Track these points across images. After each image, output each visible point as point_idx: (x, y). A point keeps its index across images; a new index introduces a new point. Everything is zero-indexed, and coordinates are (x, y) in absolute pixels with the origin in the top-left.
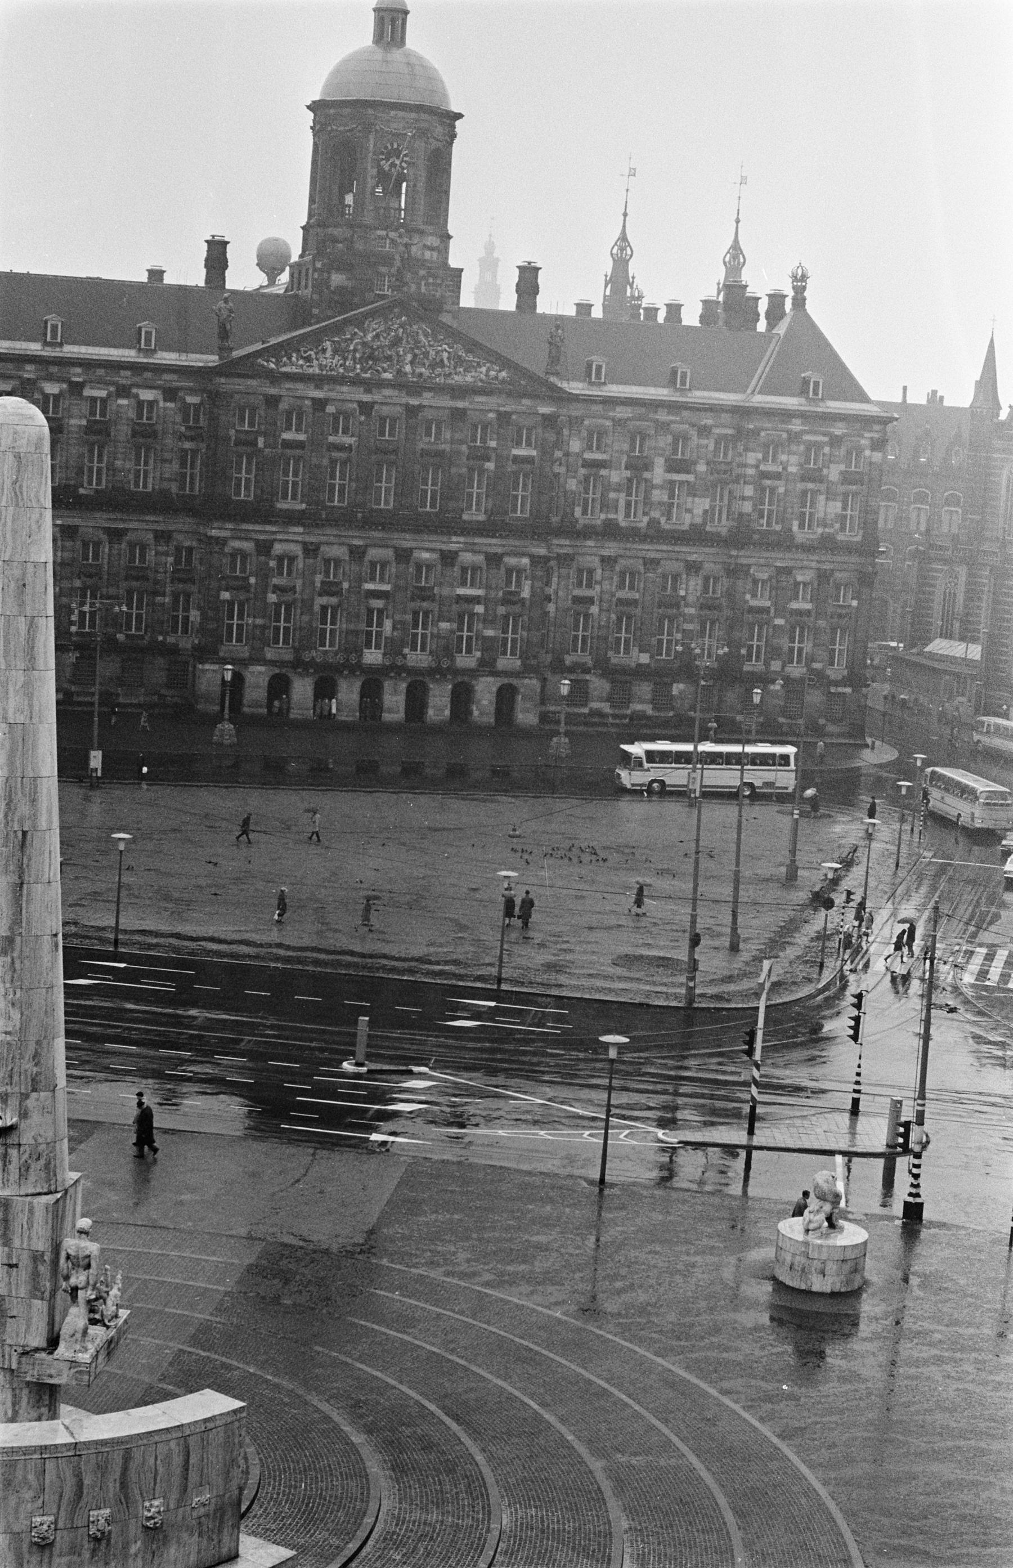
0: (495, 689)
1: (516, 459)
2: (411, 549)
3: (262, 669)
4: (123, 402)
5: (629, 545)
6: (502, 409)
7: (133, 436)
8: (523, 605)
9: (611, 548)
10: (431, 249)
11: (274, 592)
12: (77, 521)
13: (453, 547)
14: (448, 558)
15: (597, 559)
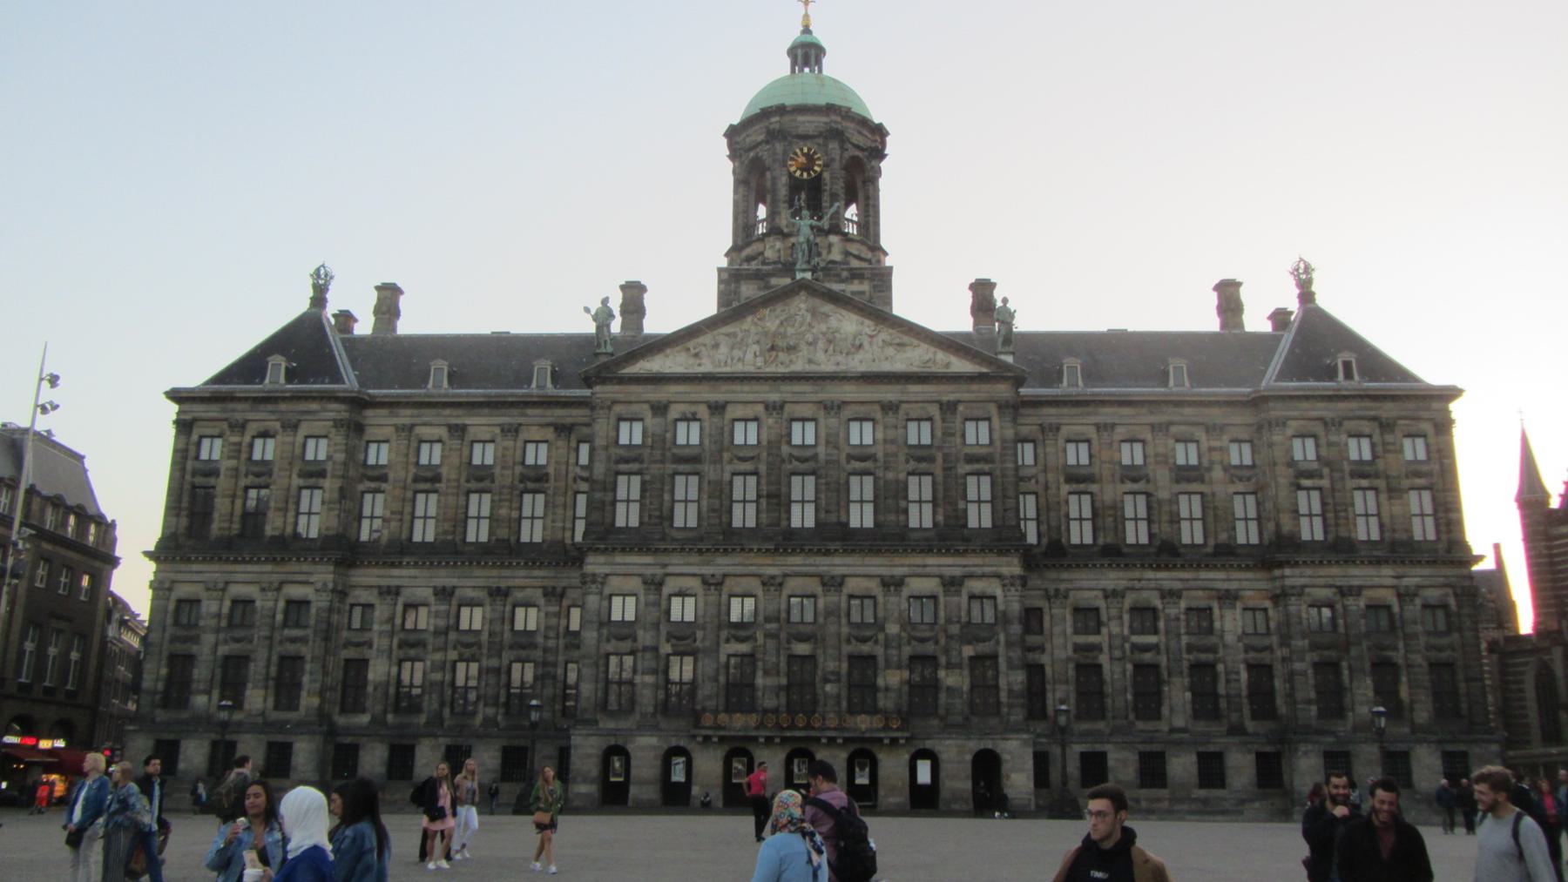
0: (969, 757)
1: (971, 459)
2: (844, 577)
3: (653, 741)
4: (510, 443)
5: (1137, 574)
6: (945, 398)
7: (521, 481)
8: (998, 643)
9: (1113, 579)
10: (858, 258)
11: (668, 641)
12: (454, 582)
13: (898, 571)
14: (893, 584)
15: (1100, 594)
